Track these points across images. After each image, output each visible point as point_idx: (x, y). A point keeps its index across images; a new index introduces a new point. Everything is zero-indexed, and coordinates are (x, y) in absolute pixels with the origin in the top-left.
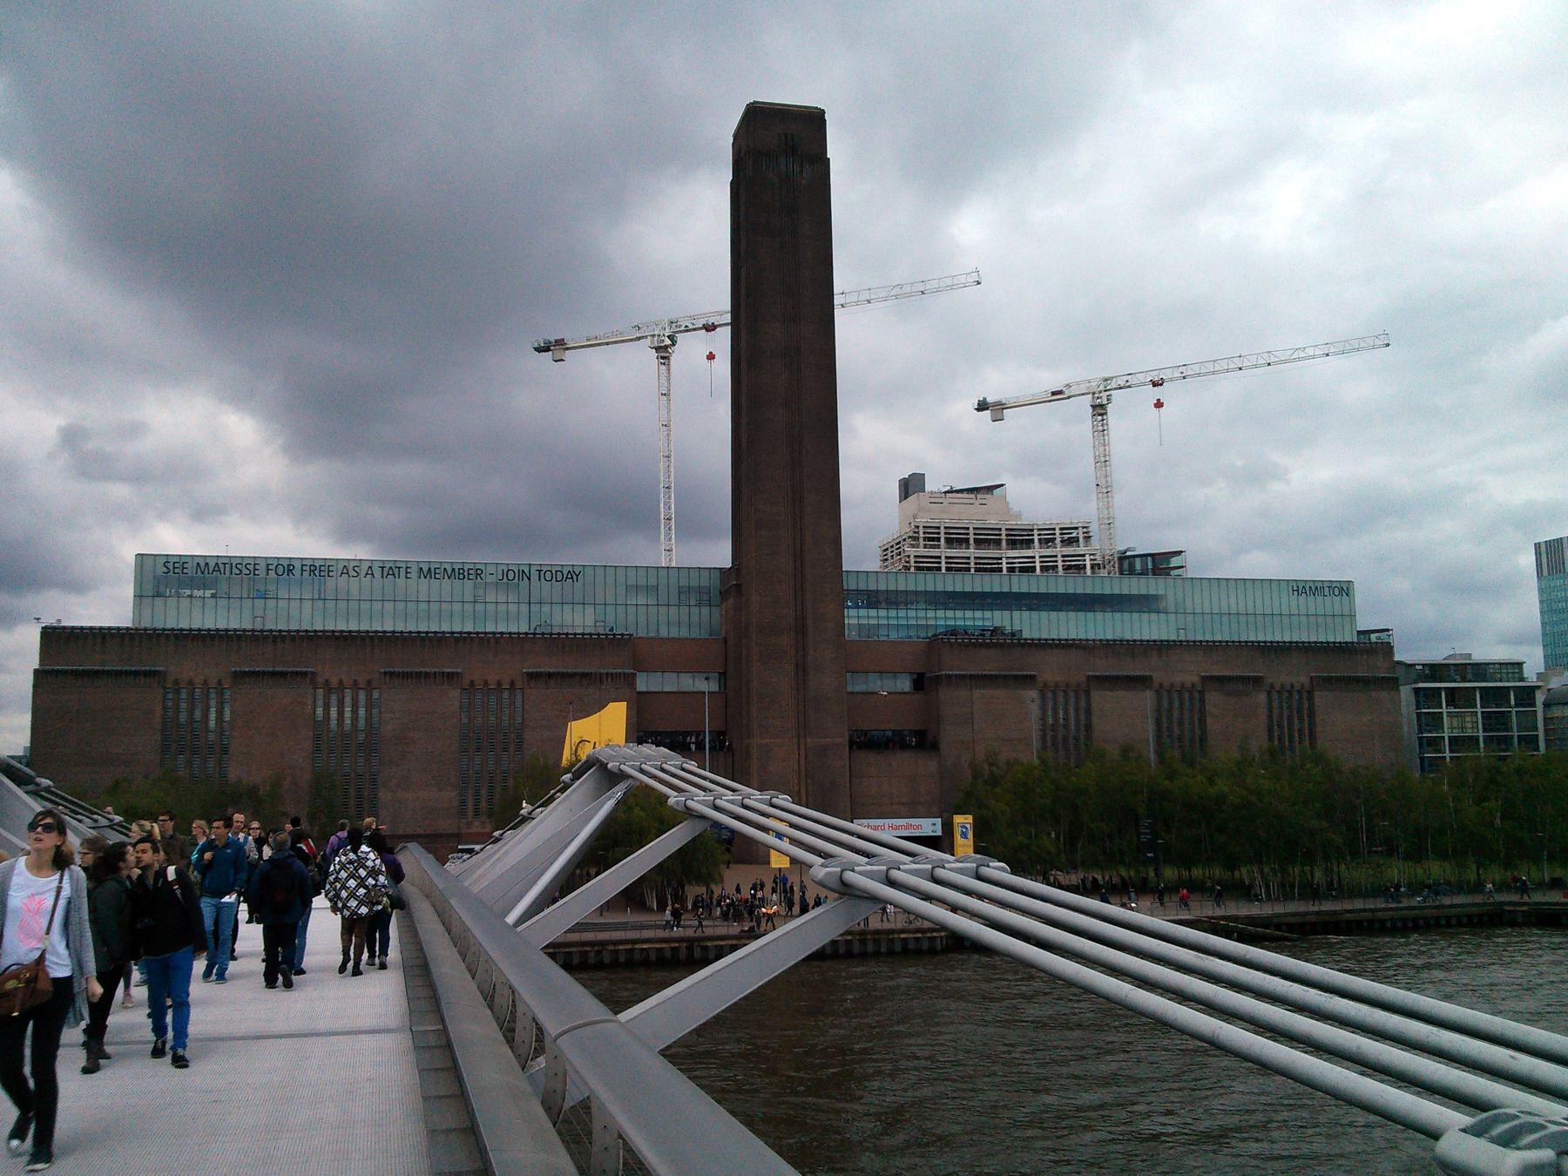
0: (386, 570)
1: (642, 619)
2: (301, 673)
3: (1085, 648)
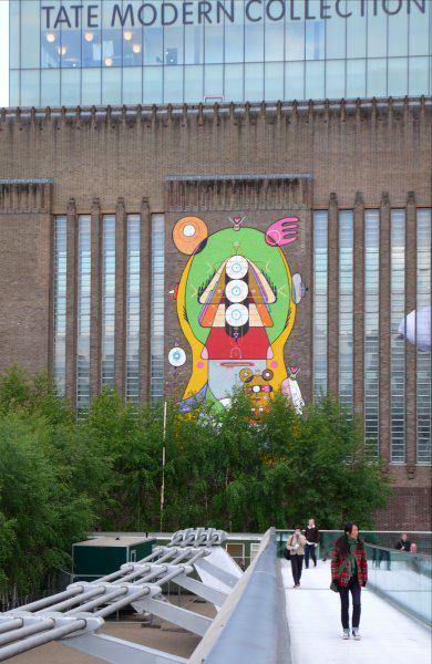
2: (287, 181)
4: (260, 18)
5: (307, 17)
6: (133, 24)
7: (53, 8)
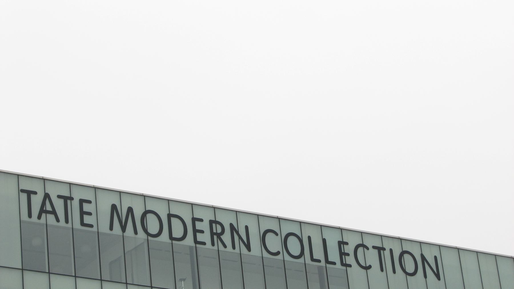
4: (278, 253)
5: (327, 261)
6: (136, 232)
7: (35, 193)
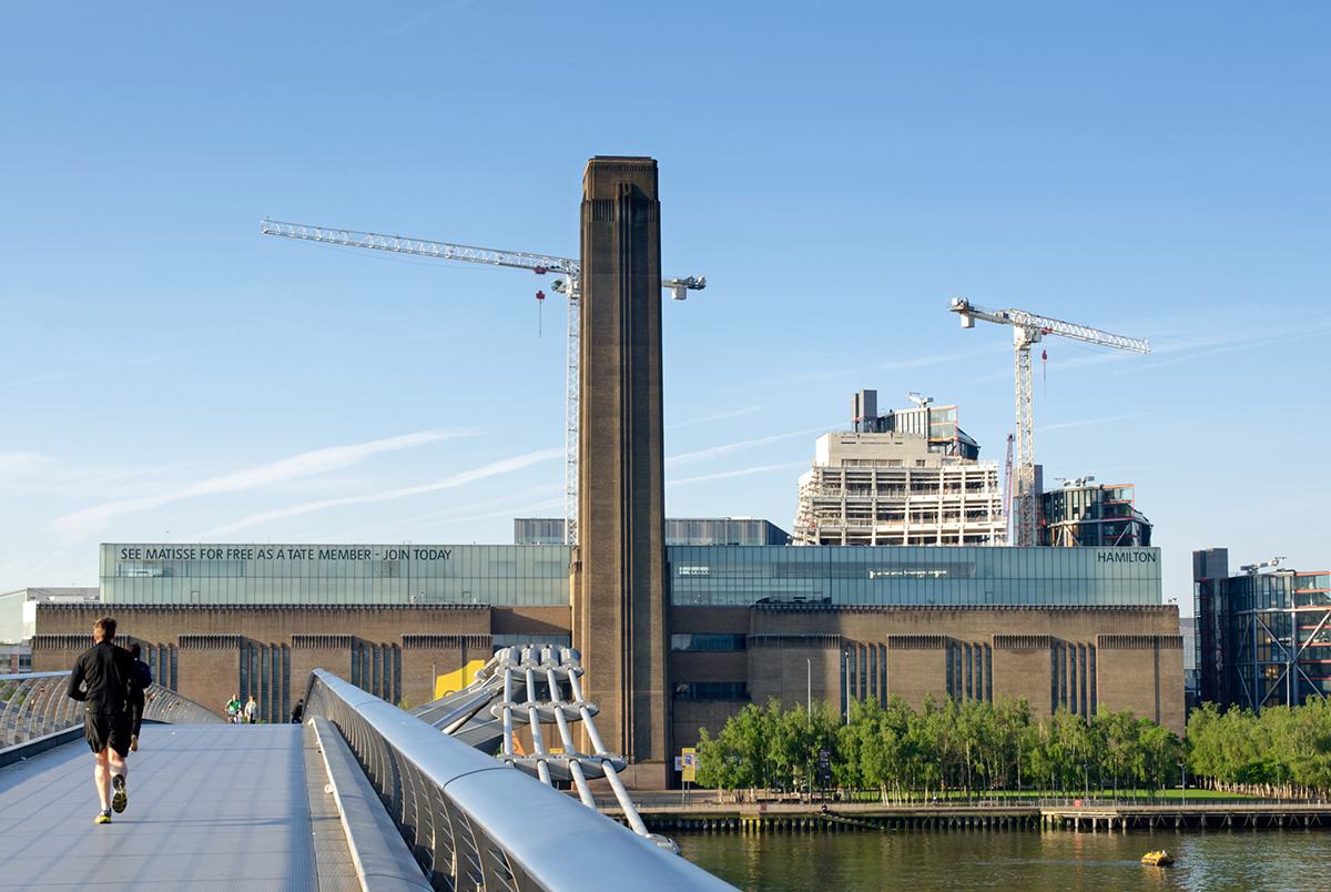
0: (293, 553)
1: (502, 589)
3: (885, 613)
